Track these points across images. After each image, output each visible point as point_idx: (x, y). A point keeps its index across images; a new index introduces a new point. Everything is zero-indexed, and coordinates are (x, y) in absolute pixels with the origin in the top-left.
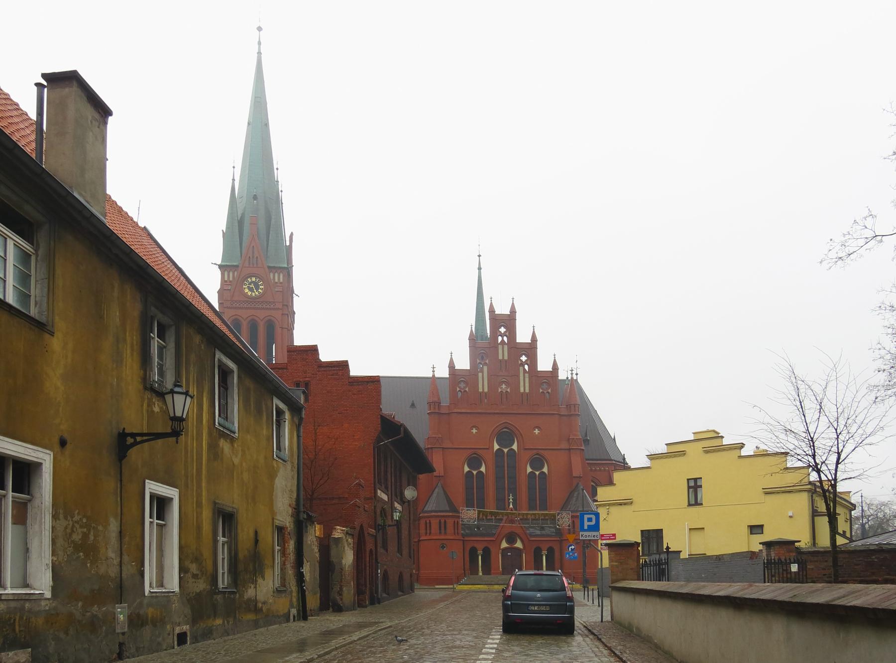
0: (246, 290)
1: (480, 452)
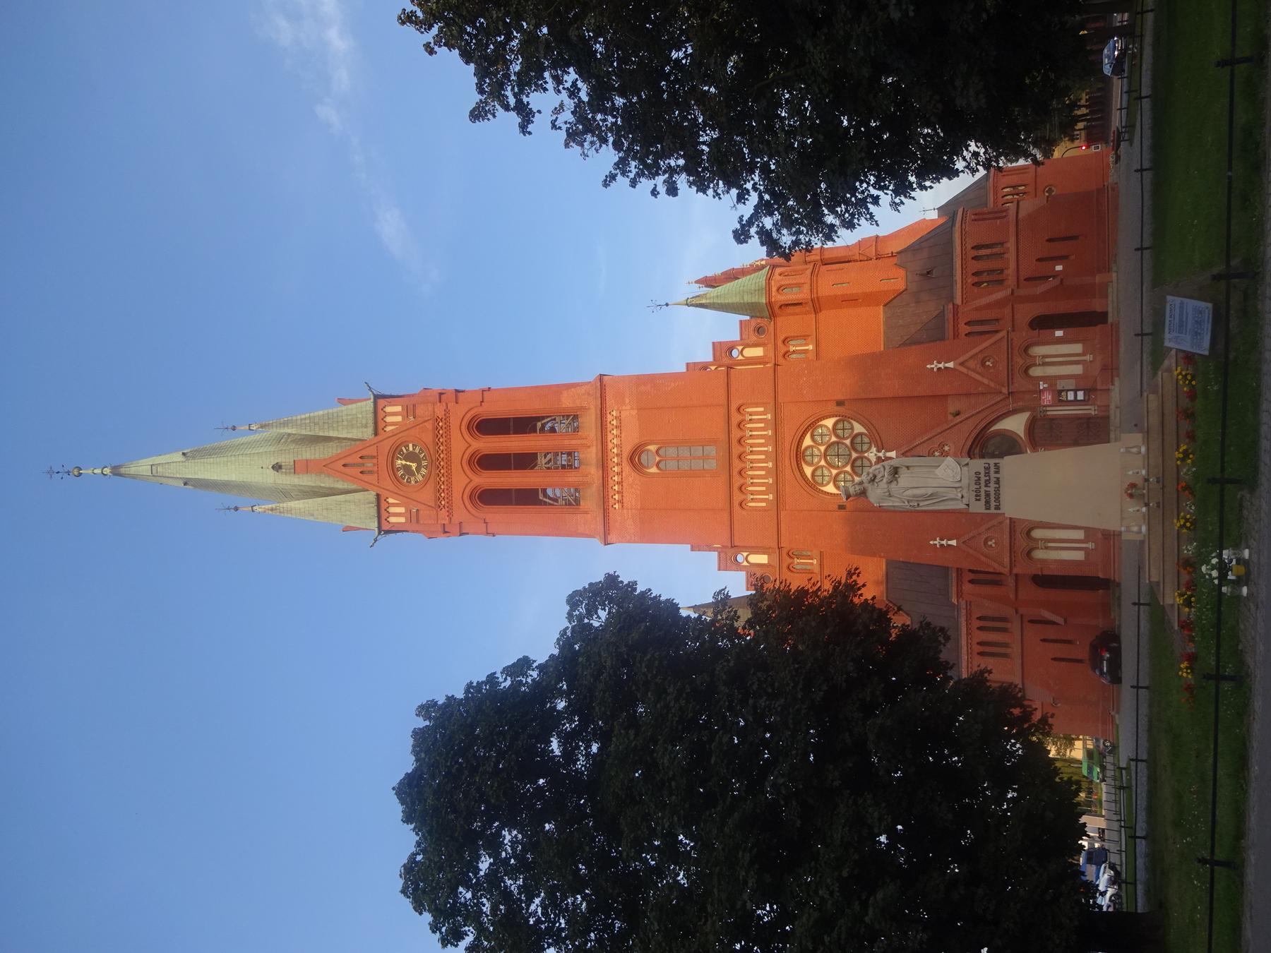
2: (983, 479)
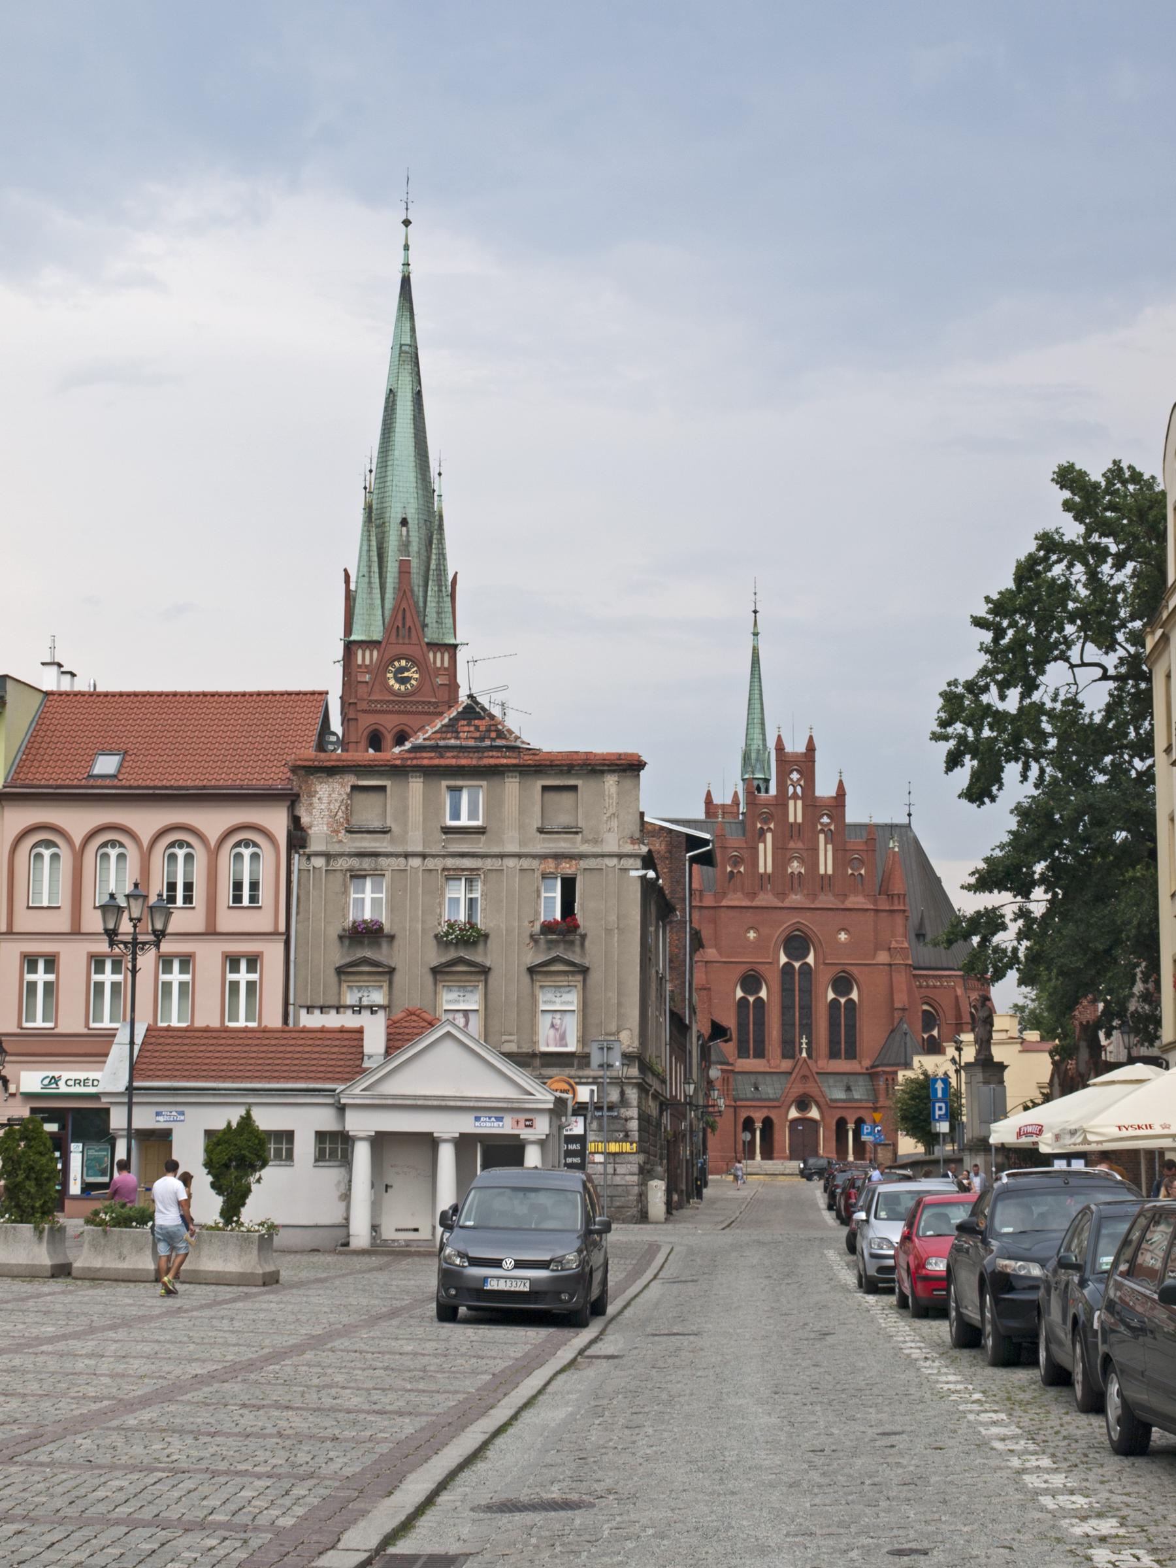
0: (392, 682)
1: (761, 968)
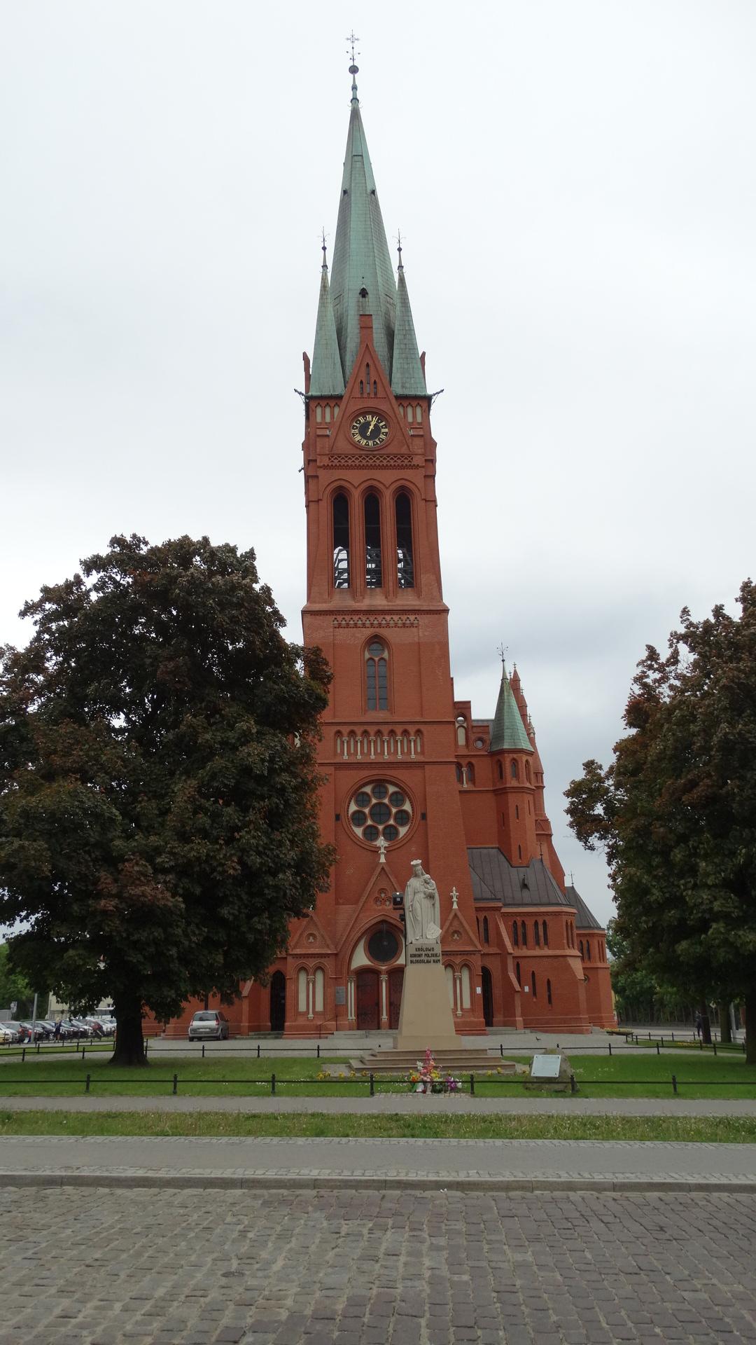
0: (358, 438)
2: (430, 953)
